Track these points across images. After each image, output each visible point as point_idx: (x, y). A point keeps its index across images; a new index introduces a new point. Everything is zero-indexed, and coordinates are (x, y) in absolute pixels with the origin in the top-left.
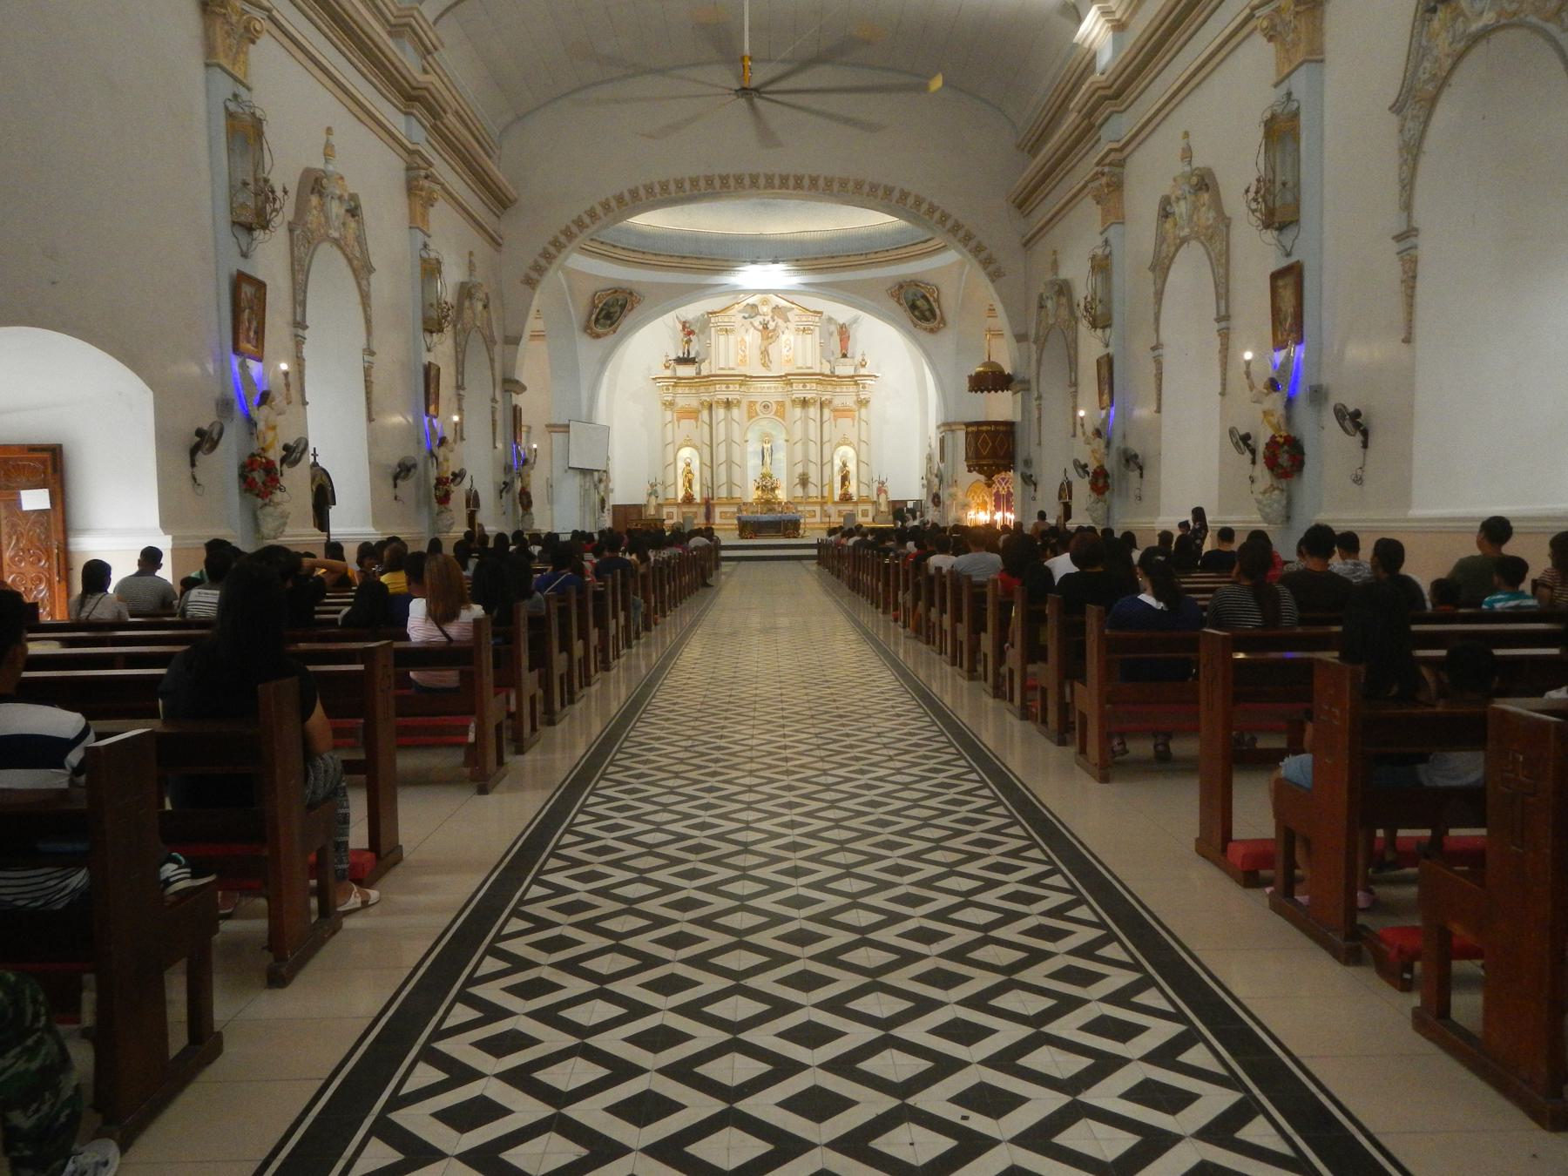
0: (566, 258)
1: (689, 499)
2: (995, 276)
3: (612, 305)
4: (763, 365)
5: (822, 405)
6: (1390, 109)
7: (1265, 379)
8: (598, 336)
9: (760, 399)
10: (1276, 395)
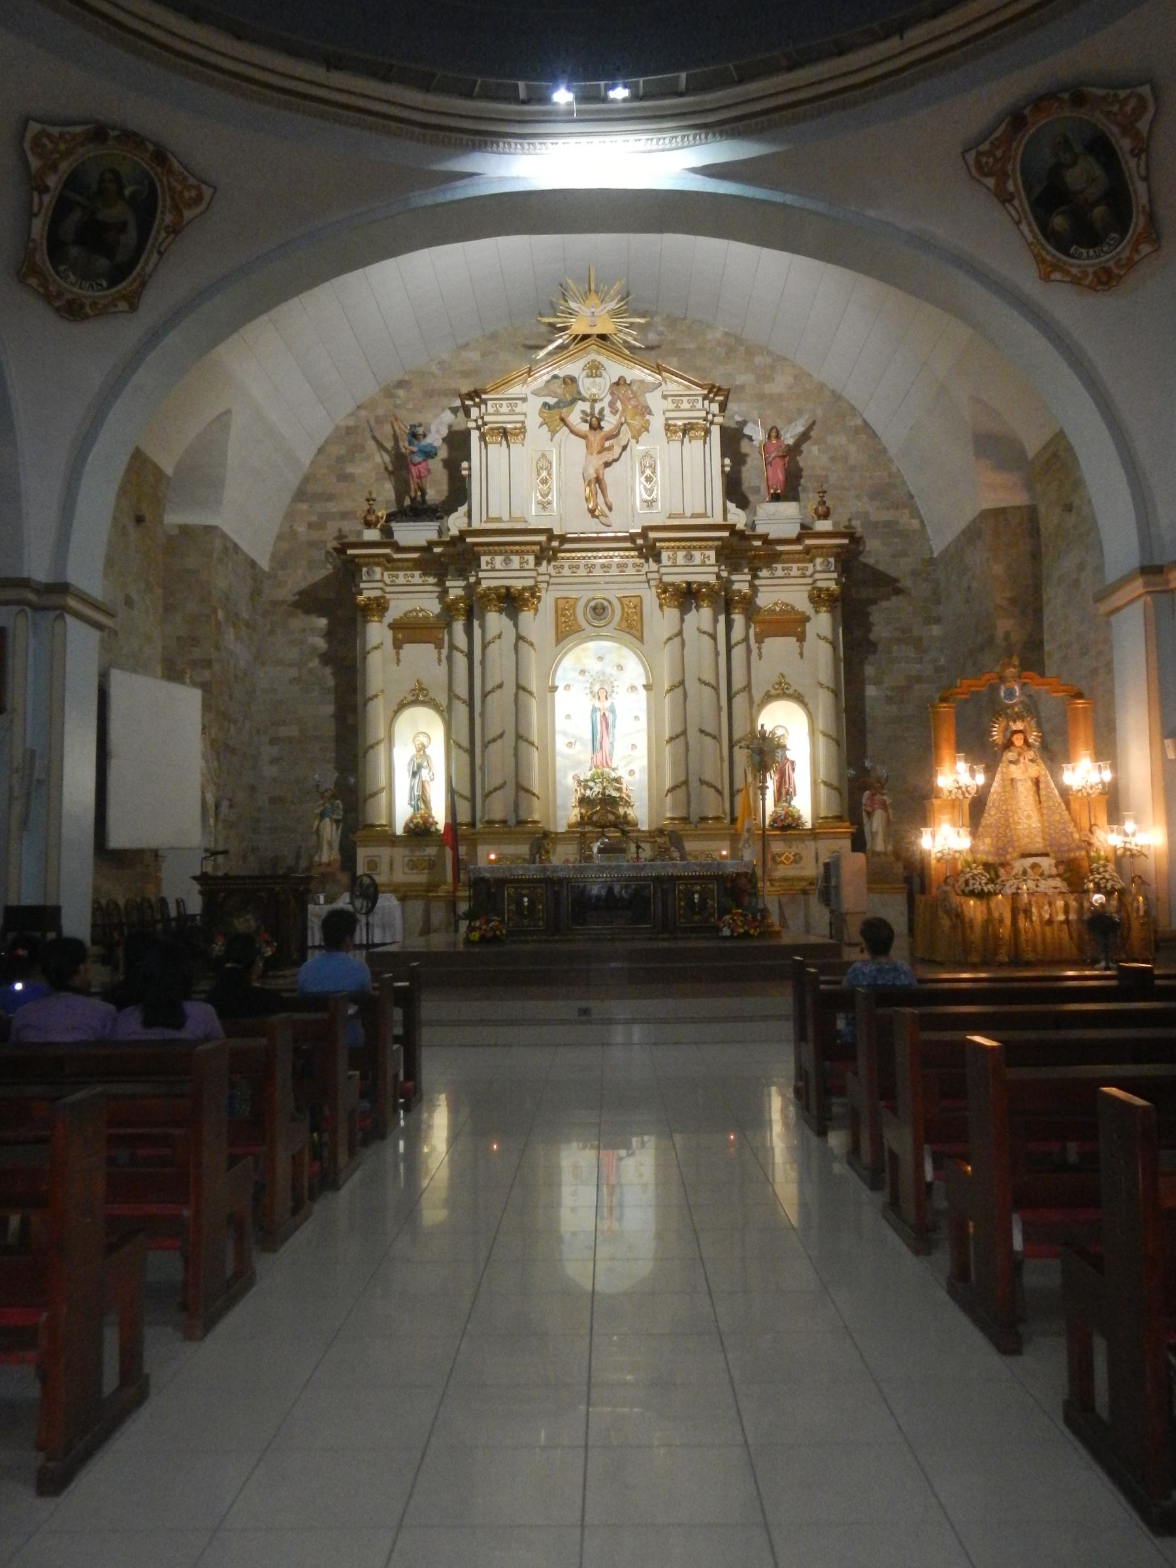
4: (592, 512)
8: (73, 311)
9: (584, 595)
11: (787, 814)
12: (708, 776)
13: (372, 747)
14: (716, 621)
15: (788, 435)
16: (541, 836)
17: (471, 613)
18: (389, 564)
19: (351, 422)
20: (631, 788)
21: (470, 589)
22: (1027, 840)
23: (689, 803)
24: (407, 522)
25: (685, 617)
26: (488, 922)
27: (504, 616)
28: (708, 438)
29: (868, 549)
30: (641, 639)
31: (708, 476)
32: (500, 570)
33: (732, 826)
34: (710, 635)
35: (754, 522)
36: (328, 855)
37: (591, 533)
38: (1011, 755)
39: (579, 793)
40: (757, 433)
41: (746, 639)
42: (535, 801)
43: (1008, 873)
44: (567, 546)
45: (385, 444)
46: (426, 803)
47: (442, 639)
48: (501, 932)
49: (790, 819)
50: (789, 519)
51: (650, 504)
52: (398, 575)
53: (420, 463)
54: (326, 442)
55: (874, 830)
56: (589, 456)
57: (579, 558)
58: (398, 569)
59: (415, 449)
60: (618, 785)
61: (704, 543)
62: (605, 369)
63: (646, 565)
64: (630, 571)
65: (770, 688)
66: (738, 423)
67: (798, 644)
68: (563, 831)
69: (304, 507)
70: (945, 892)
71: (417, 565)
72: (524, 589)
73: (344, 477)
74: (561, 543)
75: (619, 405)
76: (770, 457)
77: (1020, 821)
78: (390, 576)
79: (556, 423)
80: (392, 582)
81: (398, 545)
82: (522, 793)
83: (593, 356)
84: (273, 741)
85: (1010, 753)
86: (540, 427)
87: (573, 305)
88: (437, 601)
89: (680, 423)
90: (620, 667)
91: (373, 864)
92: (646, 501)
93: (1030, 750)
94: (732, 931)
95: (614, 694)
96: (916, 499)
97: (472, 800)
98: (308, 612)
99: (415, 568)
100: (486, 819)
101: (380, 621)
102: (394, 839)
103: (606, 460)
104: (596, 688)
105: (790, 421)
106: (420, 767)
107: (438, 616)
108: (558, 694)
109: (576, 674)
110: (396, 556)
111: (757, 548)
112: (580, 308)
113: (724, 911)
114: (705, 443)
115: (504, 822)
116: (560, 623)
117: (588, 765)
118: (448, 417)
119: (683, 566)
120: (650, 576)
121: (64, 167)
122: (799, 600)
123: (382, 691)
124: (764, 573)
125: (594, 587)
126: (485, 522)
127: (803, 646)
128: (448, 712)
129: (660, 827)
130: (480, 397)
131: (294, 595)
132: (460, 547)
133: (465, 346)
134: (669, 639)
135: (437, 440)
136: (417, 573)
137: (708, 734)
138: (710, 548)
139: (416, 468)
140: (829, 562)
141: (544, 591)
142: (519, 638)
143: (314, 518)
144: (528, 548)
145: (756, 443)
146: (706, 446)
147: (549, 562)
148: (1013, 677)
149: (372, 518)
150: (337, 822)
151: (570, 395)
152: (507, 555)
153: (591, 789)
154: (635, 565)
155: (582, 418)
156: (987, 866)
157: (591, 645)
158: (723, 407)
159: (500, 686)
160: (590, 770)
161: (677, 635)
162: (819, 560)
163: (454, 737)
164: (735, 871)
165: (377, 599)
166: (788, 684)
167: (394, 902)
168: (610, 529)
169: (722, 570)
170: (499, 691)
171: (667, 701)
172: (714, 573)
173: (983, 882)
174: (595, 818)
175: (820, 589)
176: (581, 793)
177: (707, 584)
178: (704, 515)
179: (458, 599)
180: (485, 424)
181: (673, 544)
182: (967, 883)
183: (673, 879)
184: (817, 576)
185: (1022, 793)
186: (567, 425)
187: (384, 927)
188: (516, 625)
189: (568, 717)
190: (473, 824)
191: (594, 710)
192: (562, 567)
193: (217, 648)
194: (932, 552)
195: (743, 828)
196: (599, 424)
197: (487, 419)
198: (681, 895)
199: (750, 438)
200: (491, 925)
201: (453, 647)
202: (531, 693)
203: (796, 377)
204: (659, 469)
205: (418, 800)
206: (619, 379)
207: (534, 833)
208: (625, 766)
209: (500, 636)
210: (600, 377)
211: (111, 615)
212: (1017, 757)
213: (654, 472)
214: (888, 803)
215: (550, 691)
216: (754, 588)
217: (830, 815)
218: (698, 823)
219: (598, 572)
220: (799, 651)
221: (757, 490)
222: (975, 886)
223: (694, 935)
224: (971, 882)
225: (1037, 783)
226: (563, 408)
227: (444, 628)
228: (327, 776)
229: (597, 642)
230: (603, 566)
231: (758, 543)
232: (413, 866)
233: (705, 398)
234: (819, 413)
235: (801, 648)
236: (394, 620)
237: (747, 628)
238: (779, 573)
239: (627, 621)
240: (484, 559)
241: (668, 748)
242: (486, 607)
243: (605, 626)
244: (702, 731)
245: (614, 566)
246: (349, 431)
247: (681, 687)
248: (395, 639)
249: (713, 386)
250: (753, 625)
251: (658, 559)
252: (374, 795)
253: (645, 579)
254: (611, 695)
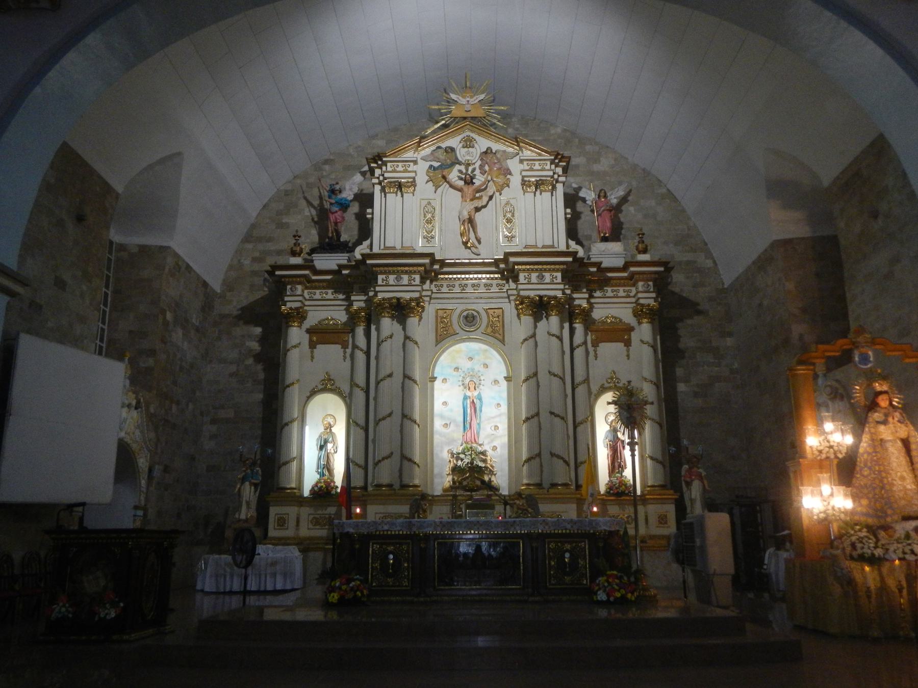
4: (465, 244)
9: (458, 308)
11: (620, 482)
12: (558, 449)
13: (287, 424)
14: (562, 328)
15: (613, 197)
16: (420, 497)
17: (369, 322)
18: (309, 283)
19: (289, 187)
20: (494, 460)
21: (369, 301)
22: (903, 502)
23: (542, 471)
24: (325, 253)
25: (537, 324)
26: (348, 581)
27: (395, 322)
28: (554, 192)
29: (674, 280)
30: (503, 341)
31: (555, 219)
32: (393, 286)
33: (578, 492)
34: (557, 337)
35: (589, 255)
36: (246, 513)
37: (465, 259)
38: (877, 416)
39: (452, 463)
40: (589, 195)
41: (585, 343)
42: (417, 468)
43: (891, 536)
44: (445, 269)
45: (314, 203)
47: (347, 341)
48: (362, 592)
49: (623, 487)
50: (617, 255)
51: (510, 239)
52: (315, 292)
53: (336, 212)
54: (269, 200)
55: (693, 497)
56: (464, 203)
57: (455, 279)
58: (316, 288)
59: (333, 201)
60: (484, 457)
61: (553, 267)
62: (477, 143)
63: (507, 285)
64: (495, 289)
65: (605, 382)
66: (575, 189)
67: (626, 347)
68: (439, 494)
69: (250, 246)
70: (835, 557)
71: (329, 285)
72: (411, 300)
73: (281, 226)
74: (441, 267)
75: (487, 168)
76: (600, 210)
77: (895, 482)
78: (309, 293)
79: (439, 180)
80: (310, 297)
81: (316, 269)
82: (406, 463)
83: (468, 133)
84: (214, 421)
85: (876, 414)
86: (426, 183)
87: (453, 96)
88: (345, 312)
89: (533, 179)
90: (486, 366)
91: (282, 522)
92: (506, 237)
93: (895, 411)
94: (608, 595)
95: (481, 386)
96: (709, 245)
97: (366, 468)
98: (247, 323)
99: (328, 288)
100: (375, 483)
101: (300, 327)
102: (300, 499)
103: (476, 205)
104: (468, 380)
105: (613, 189)
106: (326, 442)
107: (345, 324)
108: (437, 384)
109: (451, 371)
110: (314, 278)
111: (592, 274)
112: (458, 98)
113: (596, 573)
114: (552, 195)
115: (390, 486)
116: (439, 329)
117: (460, 442)
118: (358, 178)
119: (536, 284)
120: (510, 292)
122: (626, 315)
123: (298, 381)
124: (598, 294)
125: (466, 301)
126: (382, 250)
127: (629, 349)
128: (349, 398)
129: (519, 491)
130: (381, 160)
131: (238, 310)
132: (362, 268)
133: (374, 137)
134: (525, 340)
135: (350, 195)
136: (330, 291)
137: (557, 416)
138: (557, 271)
139: (333, 215)
140: (649, 285)
141: (427, 303)
142: (407, 338)
143: (257, 254)
144: (415, 268)
145: (589, 203)
146: (553, 197)
147: (431, 282)
148: (866, 342)
149: (298, 249)
150: (256, 485)
151: (450, 160)
152: (398, 274)
153: (462, 460)
154: (498, 285)
155: (458, 177)
156: (872, 530)
157: (464, 347)
158: (565, 170)
159: (390, 375)
160: (461, 446)
161: (531, 337)
162: (640, 284)
163: (353, 417)
164: (607, 529)
165: (297, 309)
166: (617, 378)
167: (294, 553)
168: (479, 257)
169: (567, 289)
170: (389, 379)
171: (524, 388)
172: (560, 290)
173: (872, 545)
174: (465, 483)
175: (642, 305)
176: (454, 464)
177: (555, 298)
178: (553, 246)
179: (360, 309)
180: (385, 179)
181: (528, 267)
182: (853, 545)
183: (542, 537)
184: (640, 295)
185: (893, 453)
186: (448, 182)
187: (285, 575)
188: (404, 329)
189: (445, 403)
190: (365, 488)
191: (465, 398)
192: (442, 286)
193: (163, 341)
194: (723, 284)
195: (587, 494)
196: (472, 181)
197: (386, 175)
198: (551, 554)
199: (584, 200)
200: (351, 585)
201: (355, 347)
202: (415, 382)
203: (616, 160)
204: (516, 214)
205: (324, 468)
206: (487, 149)
207: (414, 495)
208: (489, 443)
209: (391, 337)
210: (473, 147)
211: (24, 283)
212: (884, 418)
213: (513, 216)
214: (703, 475)
215: (430, 381)
216: (591, 306)
217: (656, 484)
218: (550, 488)
219: (469, 289)
220: (625, 353)
221: (589, 238)
222: (866, 550)
223: (565, 598)
224: (859, 545)
225: (906, 443)
226: (444, 169)
227: (350, 333)
228: (251, 448)
229: (468, 343)
230: (473, 285)
231: (594, 269)
232: (316, 522)
233: (552, 162)
234: (634, 183)
235: (628, 351)
236: (311, 326)
237: (586, 335)
238: (610, 294)
239: (492, 327)
240: (380, 277)
241: (524, 427)
242: (381, 314)
243: (472, 331)
244: (552, 413)
245: (482, 286)
246: (287, 193)
247: (535, 379)
248: (311, 341)
249: (558, 154)
250: (590, 333)
251: (516, 279)
252: (287, 463)
253: (506, 296)
254: (478, 387)
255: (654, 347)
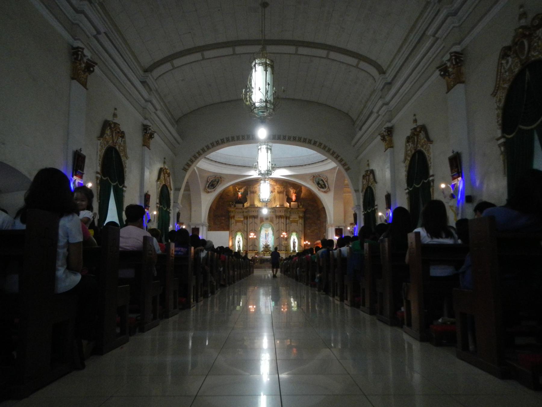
0: (199, 161)
1: (239, 251)
2: (347, 170)
3: (214, 182)
5: (286, 218)
6: (491, 95)
7: (450, 194)
8: (208, 192)
10: (454, 200)
41: (289, 223)
46: (240, 247)
121: (211, 180)
142: (255, 223)
165: (233, 216)
177: (283, 216)
191: (266, 233)
201: (245, 223)
255: (302, 224)
